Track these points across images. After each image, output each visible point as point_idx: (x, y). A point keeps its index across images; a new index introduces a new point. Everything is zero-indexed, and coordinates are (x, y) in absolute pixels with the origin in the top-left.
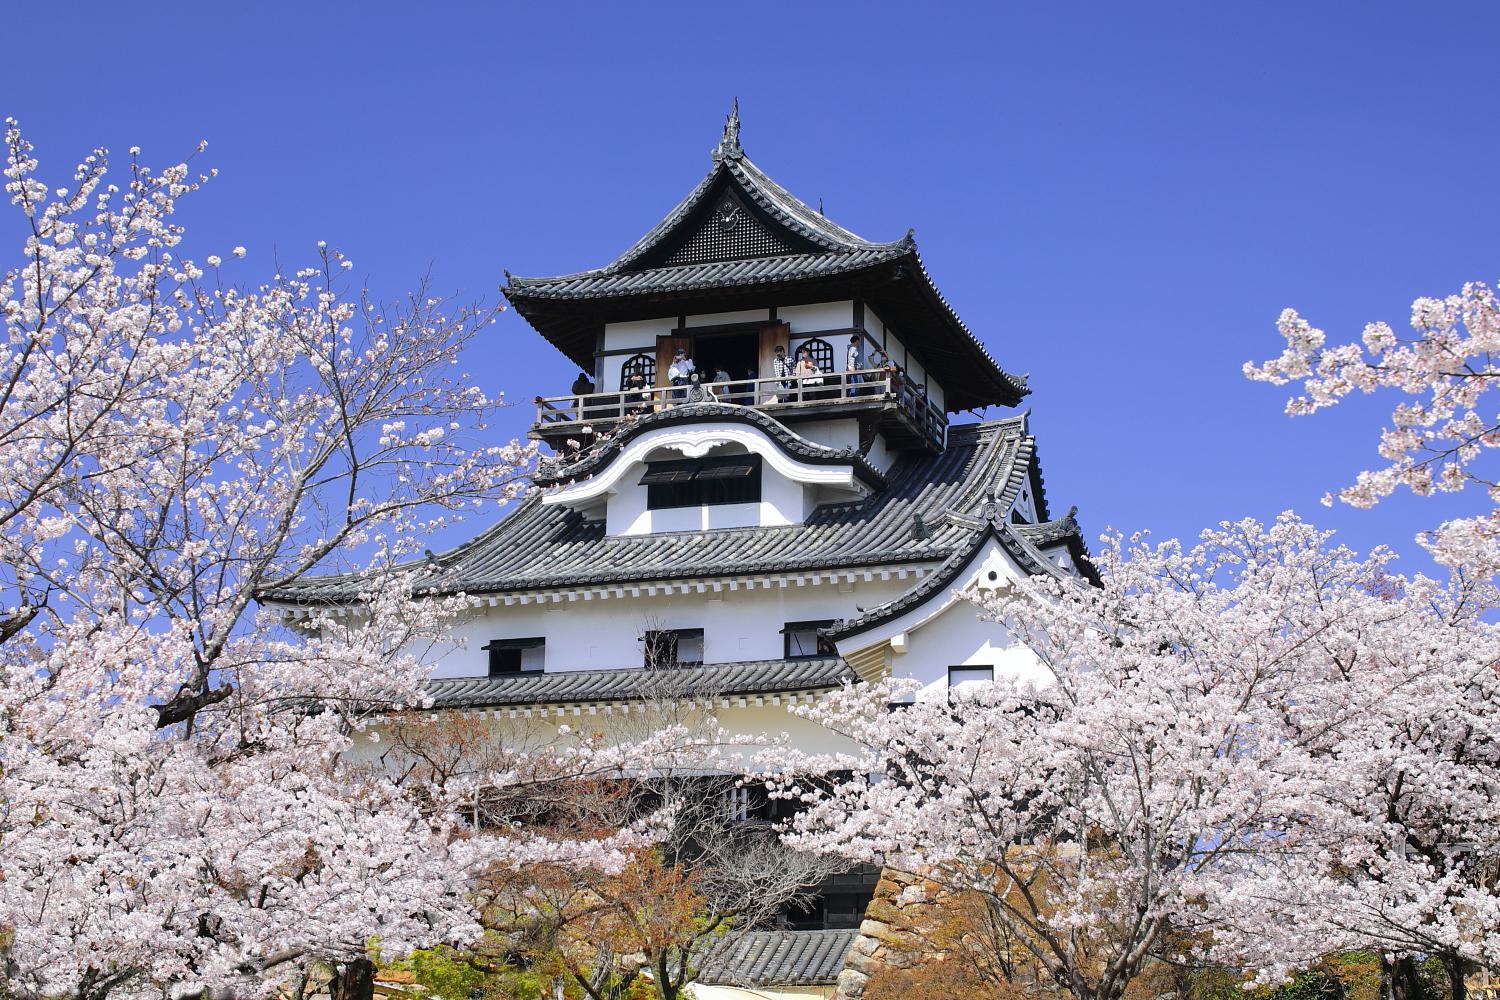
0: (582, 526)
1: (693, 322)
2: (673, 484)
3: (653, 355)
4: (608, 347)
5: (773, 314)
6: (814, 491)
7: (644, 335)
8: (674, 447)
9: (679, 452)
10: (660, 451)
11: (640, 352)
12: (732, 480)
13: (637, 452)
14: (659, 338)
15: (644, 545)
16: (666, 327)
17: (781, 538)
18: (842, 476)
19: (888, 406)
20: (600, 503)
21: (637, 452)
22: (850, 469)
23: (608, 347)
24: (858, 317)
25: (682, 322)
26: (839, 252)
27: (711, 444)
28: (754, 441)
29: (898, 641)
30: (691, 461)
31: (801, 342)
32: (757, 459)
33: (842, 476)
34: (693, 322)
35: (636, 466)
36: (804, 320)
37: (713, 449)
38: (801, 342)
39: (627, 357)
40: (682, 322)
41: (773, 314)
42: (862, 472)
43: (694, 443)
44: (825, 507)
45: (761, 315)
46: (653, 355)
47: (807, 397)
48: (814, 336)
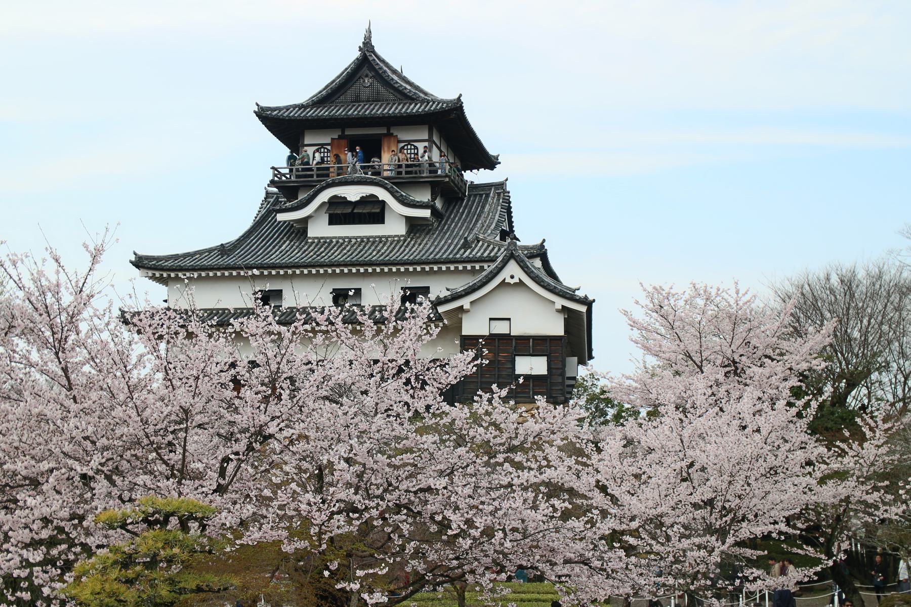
0: (299, 230)
1: (349, 132)
2: (341, 212)
3: (329, 147)
4: (306, 142)
5: (389, 130)
6: (409, 220)
9: (345, 198)
10: (335, 197)
11: (322, 145)
12: (372, 212)
13: (325, 196)
14: (332, 139)
15: (326, 243)
17: (394, 241)
18: (426, 213)
19: (447, 179)
20: (305, 221)
21: (325, 196)
23: (306, 142)
24: (431, 135)
25: (343, 132)
26: (423, 101)
28: (382, 194)
30: (350, 202)
31: (403, 144)
32: (383, 203)
33: (426, 213)
34: (349, 132)
36: (404, 135)
37: (362, 198)
38: (403, 144)
40: (343, 132)
41: (389, 130)
42: (435, 212)
43: (353, 193)
44: (414, 225)
45: (384, 131)
46: (329, 147)
47: (407, 173)
48: (409, 142)
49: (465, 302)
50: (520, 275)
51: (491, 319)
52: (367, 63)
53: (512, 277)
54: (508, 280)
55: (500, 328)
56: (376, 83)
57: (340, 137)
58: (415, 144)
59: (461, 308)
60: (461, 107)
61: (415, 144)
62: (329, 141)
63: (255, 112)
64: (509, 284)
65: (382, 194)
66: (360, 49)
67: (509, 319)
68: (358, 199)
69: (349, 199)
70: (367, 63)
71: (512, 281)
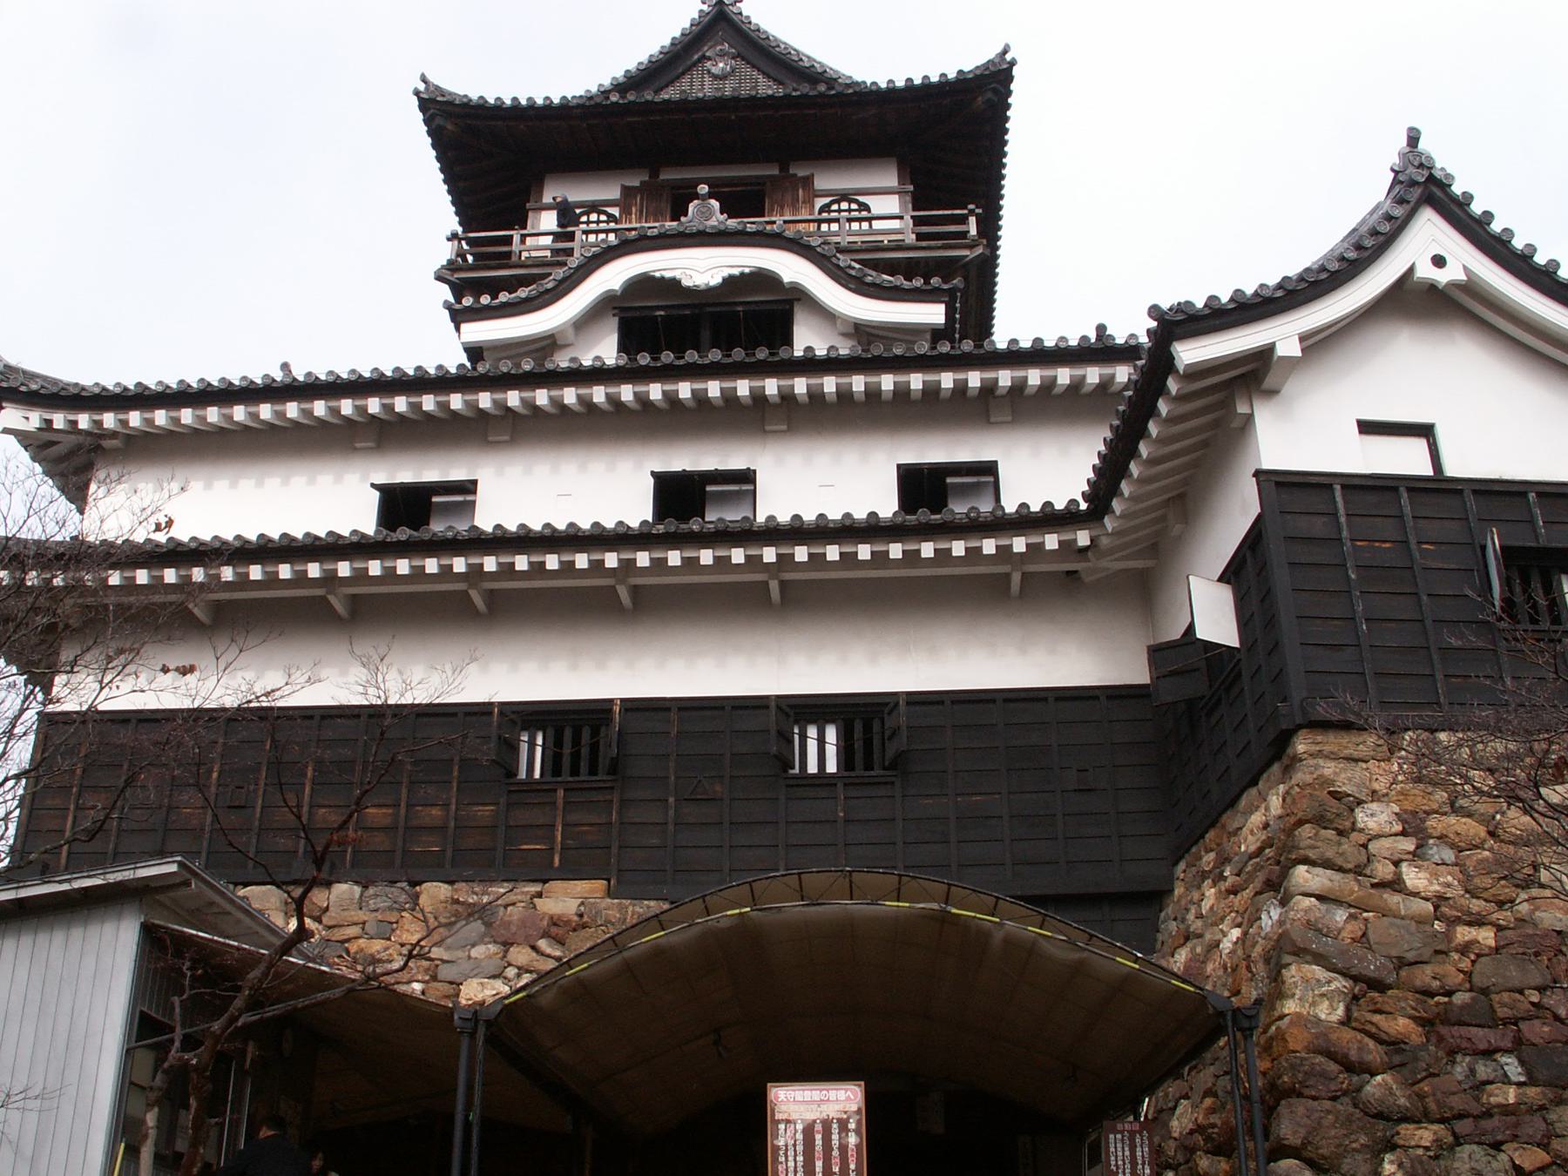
3: (615, 211)
5: (784, 168)
8: (668, 275)
9: (674, 283)
10: (643, 284)
21: (613, 276)
25: (654, 174)
27: (726, 272)
28: (791, 268)
29: (1289, 348)
34: (667, 175)
35: (607, 304)
37: (729, 281)
38: (827, 200)
40: (654, 174)
41: (784, 168)
43: (701, 268)
46: (615, 211)
48: (844, 196)
49: (1283, 334)
51: (1368, 428)
53: (1439, 261)
54: (1426, 271)
57: (644, 189)
58: (861, 199)
59: (1264, 355)
60: (1010, 79)
61: (861, 199)
62: (614, 193)
63: (417, 93)
64: (1432, 288)
65: (791, 268)
67: (1424, 431)
69: (686, 282)
70: (721, 26)
71: (1442, 277)
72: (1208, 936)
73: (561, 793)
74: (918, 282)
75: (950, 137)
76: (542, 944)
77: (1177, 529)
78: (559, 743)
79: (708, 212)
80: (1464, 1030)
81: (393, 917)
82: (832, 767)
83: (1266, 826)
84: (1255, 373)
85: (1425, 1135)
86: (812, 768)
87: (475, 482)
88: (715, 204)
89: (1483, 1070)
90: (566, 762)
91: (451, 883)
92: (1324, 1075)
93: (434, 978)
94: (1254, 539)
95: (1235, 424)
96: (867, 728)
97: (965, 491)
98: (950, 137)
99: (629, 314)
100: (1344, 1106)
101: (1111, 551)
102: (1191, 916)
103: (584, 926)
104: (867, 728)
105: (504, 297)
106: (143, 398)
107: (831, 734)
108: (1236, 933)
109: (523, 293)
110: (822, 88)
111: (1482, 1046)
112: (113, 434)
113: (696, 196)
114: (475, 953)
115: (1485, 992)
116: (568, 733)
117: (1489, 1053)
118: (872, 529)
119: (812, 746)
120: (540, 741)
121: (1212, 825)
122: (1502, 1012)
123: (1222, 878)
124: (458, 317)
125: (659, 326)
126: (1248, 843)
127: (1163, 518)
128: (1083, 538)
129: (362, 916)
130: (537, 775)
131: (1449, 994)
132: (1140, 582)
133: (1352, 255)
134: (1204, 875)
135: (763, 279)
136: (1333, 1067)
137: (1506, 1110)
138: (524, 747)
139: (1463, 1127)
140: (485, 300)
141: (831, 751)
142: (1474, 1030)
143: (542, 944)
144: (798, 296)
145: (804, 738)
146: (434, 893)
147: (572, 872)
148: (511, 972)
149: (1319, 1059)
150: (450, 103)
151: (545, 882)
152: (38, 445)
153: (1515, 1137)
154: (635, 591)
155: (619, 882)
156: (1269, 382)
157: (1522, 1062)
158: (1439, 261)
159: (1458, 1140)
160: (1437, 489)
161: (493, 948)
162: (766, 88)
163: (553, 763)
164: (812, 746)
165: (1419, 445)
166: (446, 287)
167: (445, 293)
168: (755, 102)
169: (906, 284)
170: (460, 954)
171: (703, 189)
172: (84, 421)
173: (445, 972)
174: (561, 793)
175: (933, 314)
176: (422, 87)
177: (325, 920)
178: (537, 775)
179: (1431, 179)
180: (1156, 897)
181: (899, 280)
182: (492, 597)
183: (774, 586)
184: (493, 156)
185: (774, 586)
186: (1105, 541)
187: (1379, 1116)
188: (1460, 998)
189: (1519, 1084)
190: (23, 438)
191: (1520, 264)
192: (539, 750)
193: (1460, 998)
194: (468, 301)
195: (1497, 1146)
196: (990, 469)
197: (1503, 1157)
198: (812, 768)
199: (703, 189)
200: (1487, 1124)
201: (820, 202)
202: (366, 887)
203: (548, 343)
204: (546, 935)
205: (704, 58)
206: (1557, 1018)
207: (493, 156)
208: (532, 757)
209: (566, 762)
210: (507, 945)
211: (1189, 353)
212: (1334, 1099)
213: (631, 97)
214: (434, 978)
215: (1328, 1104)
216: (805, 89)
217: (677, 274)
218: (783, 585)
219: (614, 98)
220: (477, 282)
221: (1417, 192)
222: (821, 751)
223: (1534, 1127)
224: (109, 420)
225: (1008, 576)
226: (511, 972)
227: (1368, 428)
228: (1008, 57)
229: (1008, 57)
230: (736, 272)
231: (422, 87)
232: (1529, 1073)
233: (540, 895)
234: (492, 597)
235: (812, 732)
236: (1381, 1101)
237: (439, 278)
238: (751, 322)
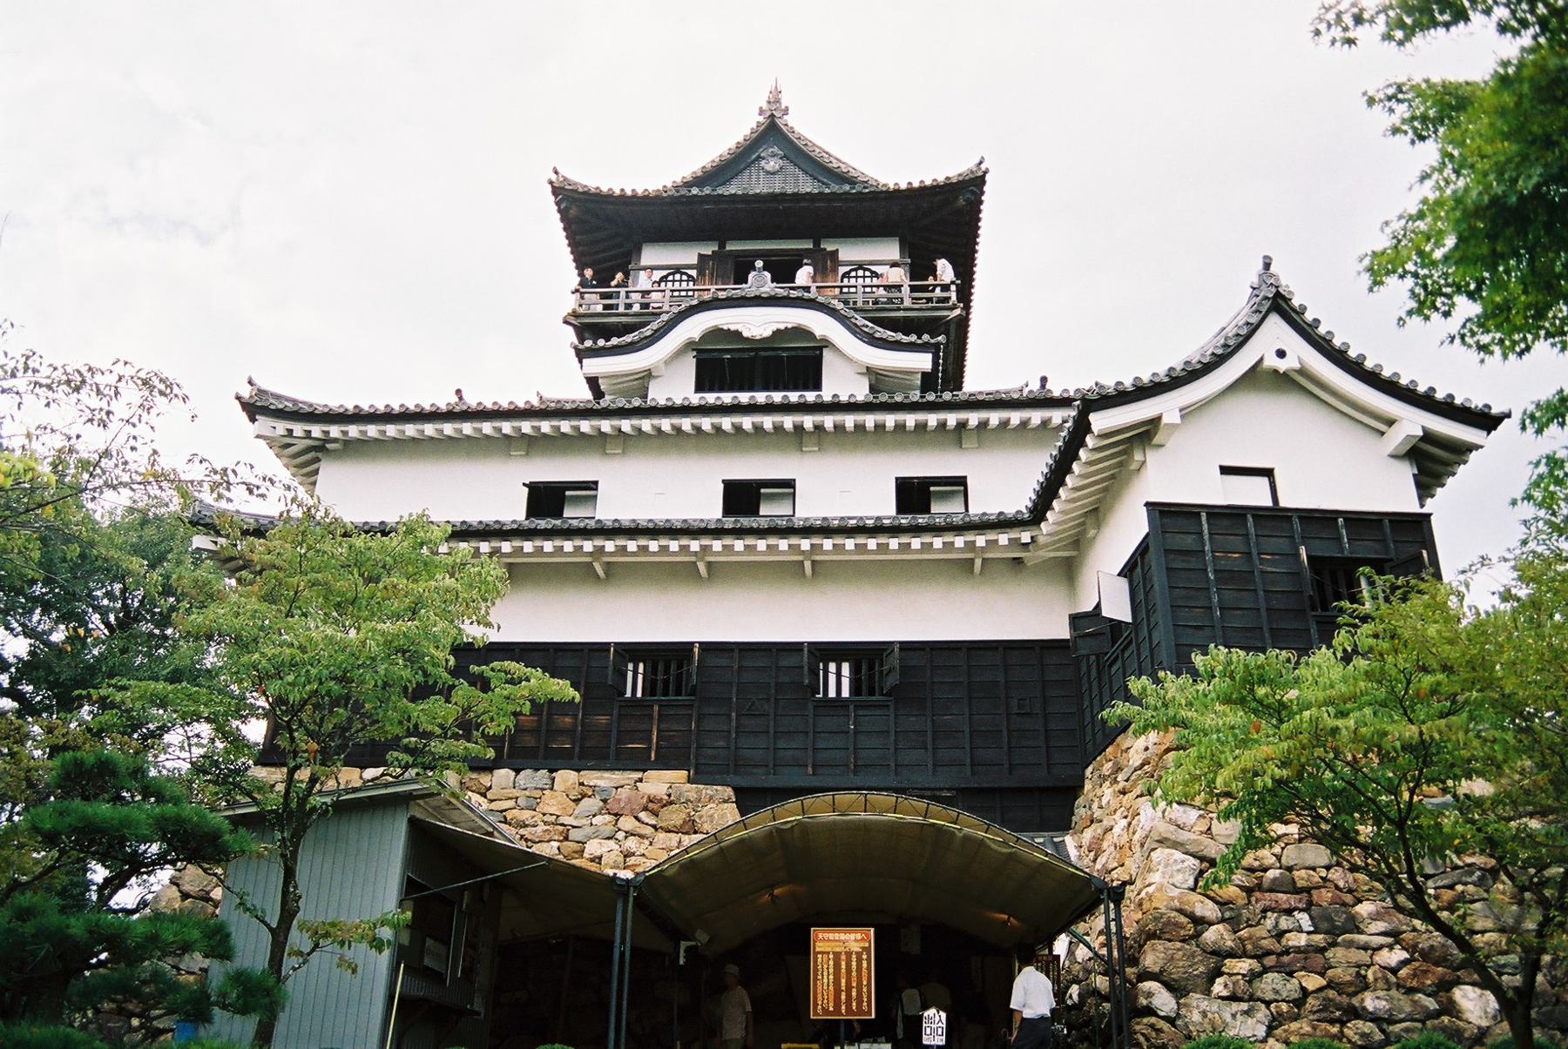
1: (732, 246)
3: (694, 273)
5: (817, 244)
6: (878, 380)
7: (687, 255)
8: (733, 328)
9: (738, 334)
10: (716, 333)
11: (678, 269)
13: (695, 327)
16: (708, 249)
21: (695, 327)
22: (930, 356)
25: (722, 246)
27: (775, 327)
28: (820, 324)
29: (1171, 417)
34: (732, 246)
35: (690, 345)
37: (777, 333)
39: (665, 273)
40: (722, 246)
41: (817, 244)
43: (757, 323)
49: (1166, 406)
50: (1301, 354)
51: (1226, 470)
52: (772, 133)
53: (1281, 354)
54: (1271, 362)
55: (1253, 494)
56: (791, 168)
59: (1155, 422)
60: (984, 182)
61: (873, 268)
62: (694, 261)
66: (761, 112)
67: (1268, 473)
68: (768, 333)
69: (746, 334)
70: (772, 133)
71: (1282, 365)
72: (1105, 822)
73: (656, 708)
74: (913, 338)
75: (941, 222)
76: (643, 815)
77: (1092, 533)
78: (655, 670)
79: (760, 282)
80: (1273, 895)
81: (537, 794)
82: (846, 693)
83: (1147, 749)
84: (1146, 433)
85: (1244, 966)
86: (832, 694)
87: (596, 483)
88: (768, 275)
89: (1285, 923)
90: (660, 685)
91: (578, 771)
92: (1177, 925)
93: (566, 839)
94: (1143, 549)
95: (1134, 466)
96: (871, 668)
97: (944, 496)
98: (941, 222)
99: (705, 356)
100: (1192, 947)
101: (1046, 546)
102: (1095, 806)
103: (671, 803)
104: (871, 668)
105: (615, 341)
106: (358, 417)
107: (846, 668)
108: (1124, 822)
109: (628, 338)
110: (847, 187)
111: (1286, 906)
112: (335, 440)
113: (754, 269)
114: (595, 821)
115: (1290, 869)
116: (661, 667)
117: (1289, 912)
118: (877, 529)
119: (832, 679)
120: (641, 669)
121: (1111, 743)
122: (1300, 883)
123: (1115, 781)
124: (581, 355)
125: (722, 365)
126: (1135, 759)
127: (1083, 524)
128: (1026, 537)
129: (516, 793)
130: (639, 694)
131: (1265, 870)
132: (1067, 568)
133: (1219, 352)
134: (1104, 778)
135: (800, 332)
136: (1183, 919)
137: (1298, 950)
138: (630, 674)
139: (1270, 961)
140: (601, 342)
141: (846, 683)
142: (1280, 895)
143: (643, 815)
144: (826, 343)
145: (826, 672)
146: (566, 778)
147: (664, 763)
148: (620, 835)
149: (1174, 914)
150: (575, 191)
151: (644, 771)
152: (282, 446)
153: (1303, 968)
154: (709, 565)
155: (696, 773)
156: (1157, 440)
157: (1312, 918)
158: (1281, 354)
159: (1266, 970)
160: (1274, 517)
161: (608, 818)
162: (807, 186)
163: (650, 687)
164: (832, 679)
165: (1264, 481)
166: (571, 329)
167: (570, 335)
168: (797, 197)
169: (905, 339)
170: (586, 822)
171: (759, 264)
172: (317, 431)
173: (574, 834)
174: (656, 708)
175: (924, 362)
176: (554, 177)
177: (489, 795)
178: (639, 694)
179: (1278, 295)
180: (1075, 789)
181: (900, 336)
182: (608, 567)
183: (808, 565)
184: (605, 231)
185: (808, 565)
186: (1041, 540)
187: (1213, 953)
188: (1271, 874)
189: (1309, 933)
190: (271, 441)
191: (1338, 357)
192: (640, 677)
193: (1271, 874)
194: (588, 343)
195: (1291, 974)
196: (961, 481)
197: (1294, 981)
198: (832, 694)
199: (759, 264)
200: (1286, 959)
201: (842, 270)
202: (518, 771)
203: (648, 375)
204: (645, 809)
205: (759, 158)
206: (1337, 887)
207: (605, 231)
208: (635, 682)
209: (660, 685)
210: (617, 815)
211: (1101, 421)
212: (1183, 941)
213: (707, 191)
214: (566, 839)
215: (1179, 945)
216: (836, 188)
217: (739, 328)
218: (813, 562)
219: (695, 191)
220: (594, 334)
221: (1267, 304)
222: (838, 681)
223: (1318, 960)
224: (335, 431)
225: (972, 560)
226: (620, 835)
227: (1226, 470)
228: (983, 167)
229: (983, 167)
230: (782, 327)
231: (554, 177)
232: (1314, 924)
233: (641, 780)
234: (608, 567)
235: (832, 667)
236: (1215, 943)
237: (566, 322)
238: (795, 363)
